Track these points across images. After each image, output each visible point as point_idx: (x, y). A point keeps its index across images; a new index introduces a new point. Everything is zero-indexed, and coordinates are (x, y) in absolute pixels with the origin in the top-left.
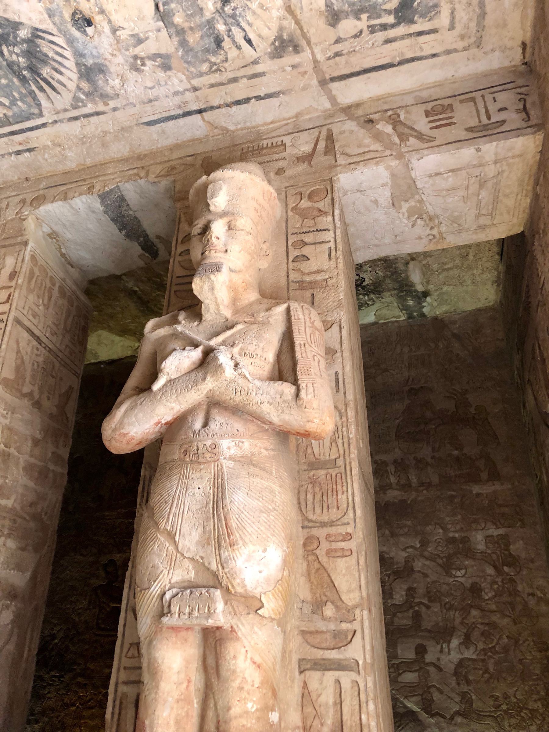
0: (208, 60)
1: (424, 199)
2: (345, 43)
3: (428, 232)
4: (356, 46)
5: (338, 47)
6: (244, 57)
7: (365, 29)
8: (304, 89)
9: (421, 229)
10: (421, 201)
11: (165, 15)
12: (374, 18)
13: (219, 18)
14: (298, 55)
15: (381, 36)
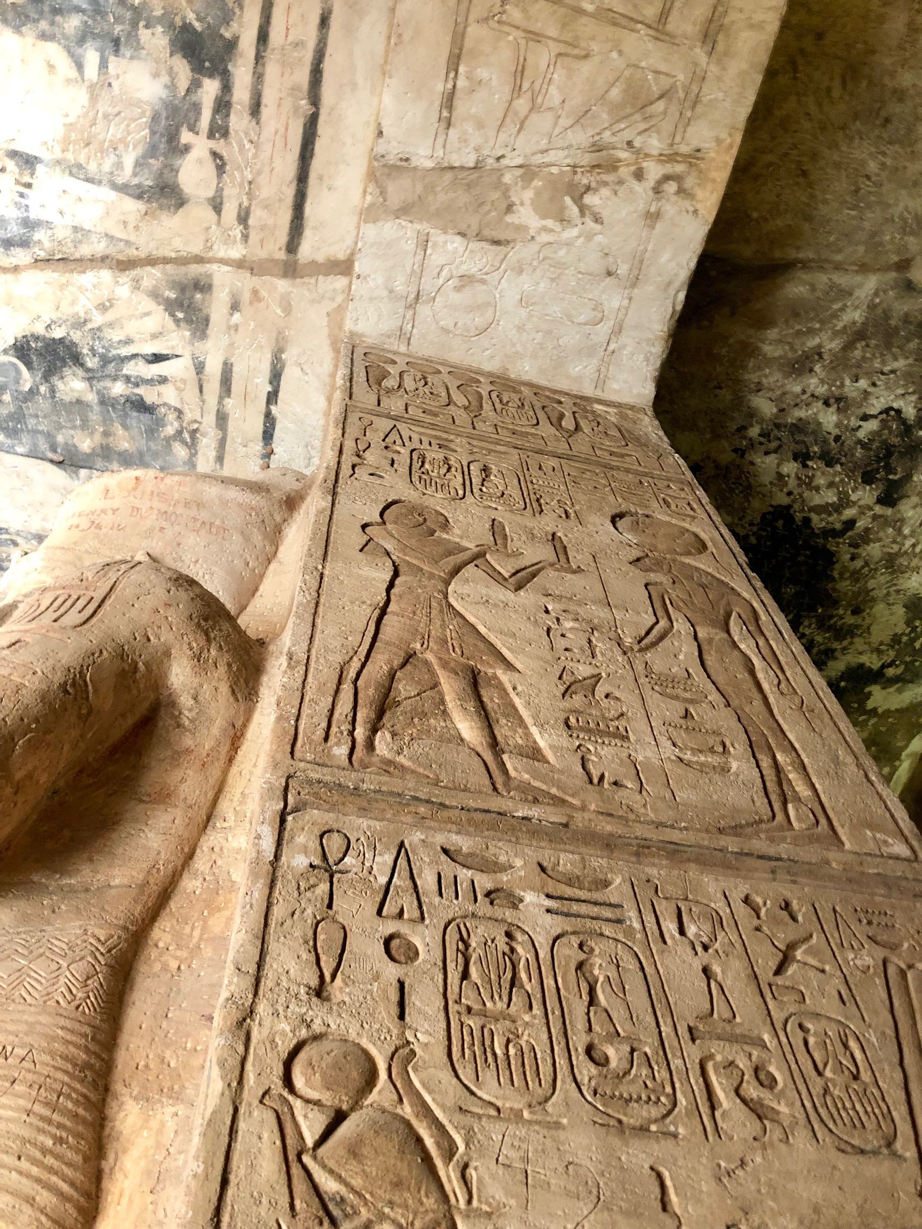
0: (168, 440)
1: (519, 161)
2: (226, 192)
3: (643, 190)
4: (243, 178)
5: (230, 210)
6: (184, 381)
7: (212, 144)
8: (288, 309)
9: (620, 205)
10: (528, 172)
11: (71, 459)
12: (197, 120)
13: (101, 384)
14: (214, 289)
15: (238, 121)
